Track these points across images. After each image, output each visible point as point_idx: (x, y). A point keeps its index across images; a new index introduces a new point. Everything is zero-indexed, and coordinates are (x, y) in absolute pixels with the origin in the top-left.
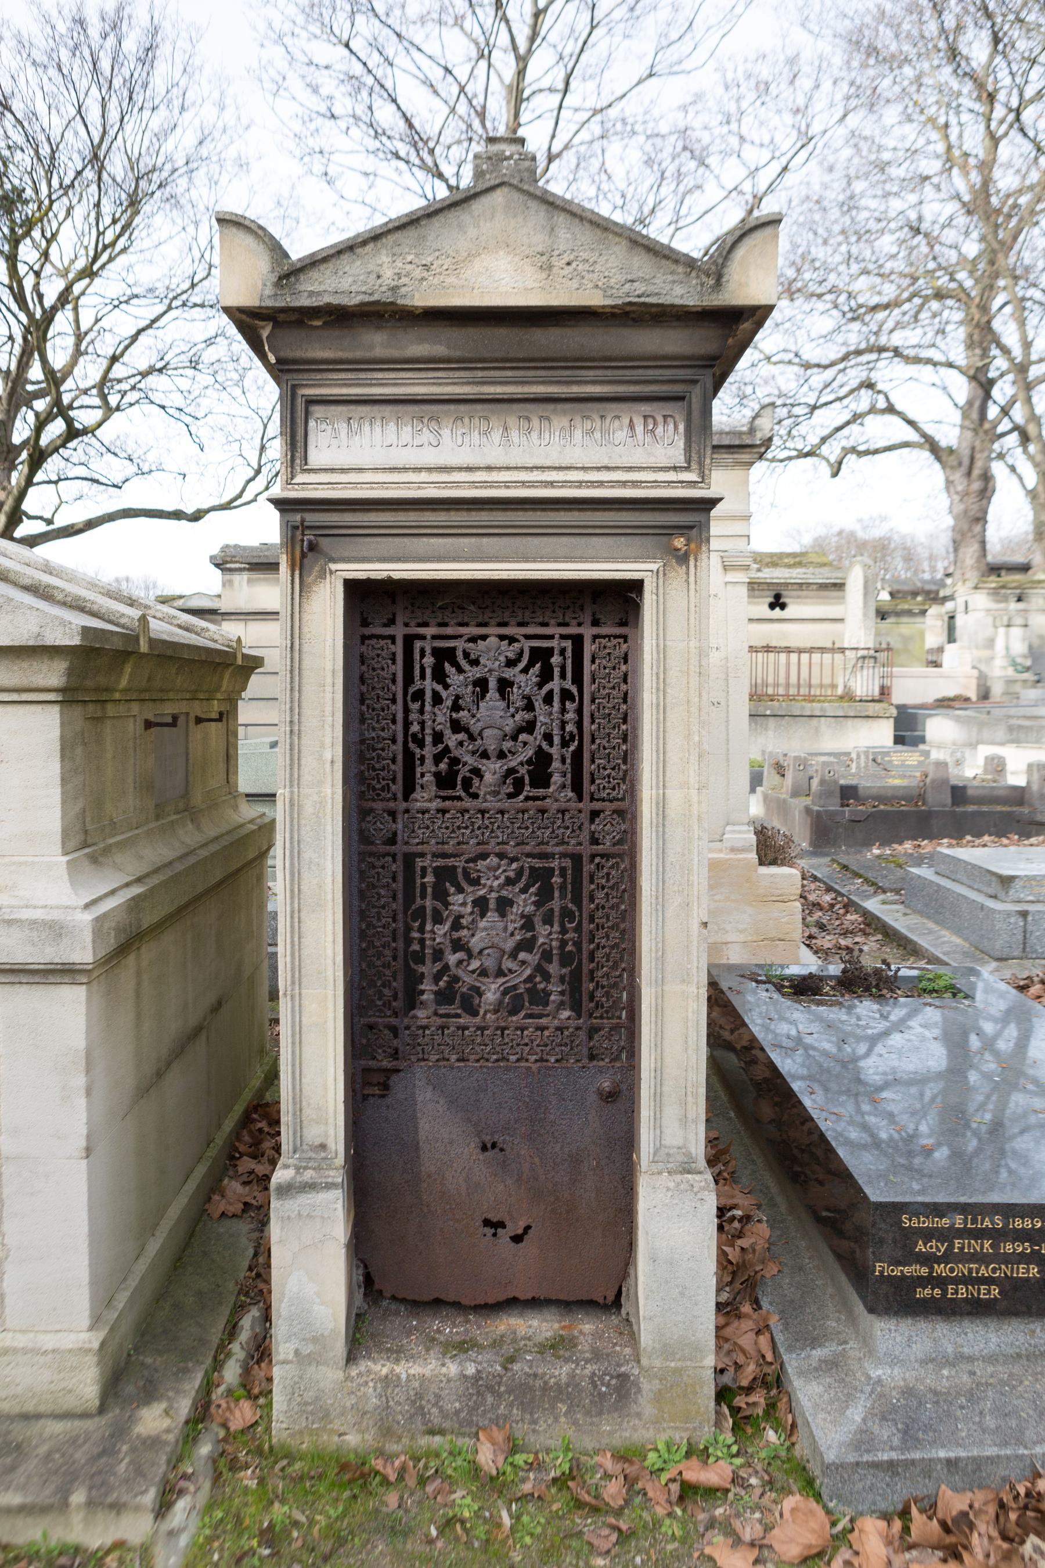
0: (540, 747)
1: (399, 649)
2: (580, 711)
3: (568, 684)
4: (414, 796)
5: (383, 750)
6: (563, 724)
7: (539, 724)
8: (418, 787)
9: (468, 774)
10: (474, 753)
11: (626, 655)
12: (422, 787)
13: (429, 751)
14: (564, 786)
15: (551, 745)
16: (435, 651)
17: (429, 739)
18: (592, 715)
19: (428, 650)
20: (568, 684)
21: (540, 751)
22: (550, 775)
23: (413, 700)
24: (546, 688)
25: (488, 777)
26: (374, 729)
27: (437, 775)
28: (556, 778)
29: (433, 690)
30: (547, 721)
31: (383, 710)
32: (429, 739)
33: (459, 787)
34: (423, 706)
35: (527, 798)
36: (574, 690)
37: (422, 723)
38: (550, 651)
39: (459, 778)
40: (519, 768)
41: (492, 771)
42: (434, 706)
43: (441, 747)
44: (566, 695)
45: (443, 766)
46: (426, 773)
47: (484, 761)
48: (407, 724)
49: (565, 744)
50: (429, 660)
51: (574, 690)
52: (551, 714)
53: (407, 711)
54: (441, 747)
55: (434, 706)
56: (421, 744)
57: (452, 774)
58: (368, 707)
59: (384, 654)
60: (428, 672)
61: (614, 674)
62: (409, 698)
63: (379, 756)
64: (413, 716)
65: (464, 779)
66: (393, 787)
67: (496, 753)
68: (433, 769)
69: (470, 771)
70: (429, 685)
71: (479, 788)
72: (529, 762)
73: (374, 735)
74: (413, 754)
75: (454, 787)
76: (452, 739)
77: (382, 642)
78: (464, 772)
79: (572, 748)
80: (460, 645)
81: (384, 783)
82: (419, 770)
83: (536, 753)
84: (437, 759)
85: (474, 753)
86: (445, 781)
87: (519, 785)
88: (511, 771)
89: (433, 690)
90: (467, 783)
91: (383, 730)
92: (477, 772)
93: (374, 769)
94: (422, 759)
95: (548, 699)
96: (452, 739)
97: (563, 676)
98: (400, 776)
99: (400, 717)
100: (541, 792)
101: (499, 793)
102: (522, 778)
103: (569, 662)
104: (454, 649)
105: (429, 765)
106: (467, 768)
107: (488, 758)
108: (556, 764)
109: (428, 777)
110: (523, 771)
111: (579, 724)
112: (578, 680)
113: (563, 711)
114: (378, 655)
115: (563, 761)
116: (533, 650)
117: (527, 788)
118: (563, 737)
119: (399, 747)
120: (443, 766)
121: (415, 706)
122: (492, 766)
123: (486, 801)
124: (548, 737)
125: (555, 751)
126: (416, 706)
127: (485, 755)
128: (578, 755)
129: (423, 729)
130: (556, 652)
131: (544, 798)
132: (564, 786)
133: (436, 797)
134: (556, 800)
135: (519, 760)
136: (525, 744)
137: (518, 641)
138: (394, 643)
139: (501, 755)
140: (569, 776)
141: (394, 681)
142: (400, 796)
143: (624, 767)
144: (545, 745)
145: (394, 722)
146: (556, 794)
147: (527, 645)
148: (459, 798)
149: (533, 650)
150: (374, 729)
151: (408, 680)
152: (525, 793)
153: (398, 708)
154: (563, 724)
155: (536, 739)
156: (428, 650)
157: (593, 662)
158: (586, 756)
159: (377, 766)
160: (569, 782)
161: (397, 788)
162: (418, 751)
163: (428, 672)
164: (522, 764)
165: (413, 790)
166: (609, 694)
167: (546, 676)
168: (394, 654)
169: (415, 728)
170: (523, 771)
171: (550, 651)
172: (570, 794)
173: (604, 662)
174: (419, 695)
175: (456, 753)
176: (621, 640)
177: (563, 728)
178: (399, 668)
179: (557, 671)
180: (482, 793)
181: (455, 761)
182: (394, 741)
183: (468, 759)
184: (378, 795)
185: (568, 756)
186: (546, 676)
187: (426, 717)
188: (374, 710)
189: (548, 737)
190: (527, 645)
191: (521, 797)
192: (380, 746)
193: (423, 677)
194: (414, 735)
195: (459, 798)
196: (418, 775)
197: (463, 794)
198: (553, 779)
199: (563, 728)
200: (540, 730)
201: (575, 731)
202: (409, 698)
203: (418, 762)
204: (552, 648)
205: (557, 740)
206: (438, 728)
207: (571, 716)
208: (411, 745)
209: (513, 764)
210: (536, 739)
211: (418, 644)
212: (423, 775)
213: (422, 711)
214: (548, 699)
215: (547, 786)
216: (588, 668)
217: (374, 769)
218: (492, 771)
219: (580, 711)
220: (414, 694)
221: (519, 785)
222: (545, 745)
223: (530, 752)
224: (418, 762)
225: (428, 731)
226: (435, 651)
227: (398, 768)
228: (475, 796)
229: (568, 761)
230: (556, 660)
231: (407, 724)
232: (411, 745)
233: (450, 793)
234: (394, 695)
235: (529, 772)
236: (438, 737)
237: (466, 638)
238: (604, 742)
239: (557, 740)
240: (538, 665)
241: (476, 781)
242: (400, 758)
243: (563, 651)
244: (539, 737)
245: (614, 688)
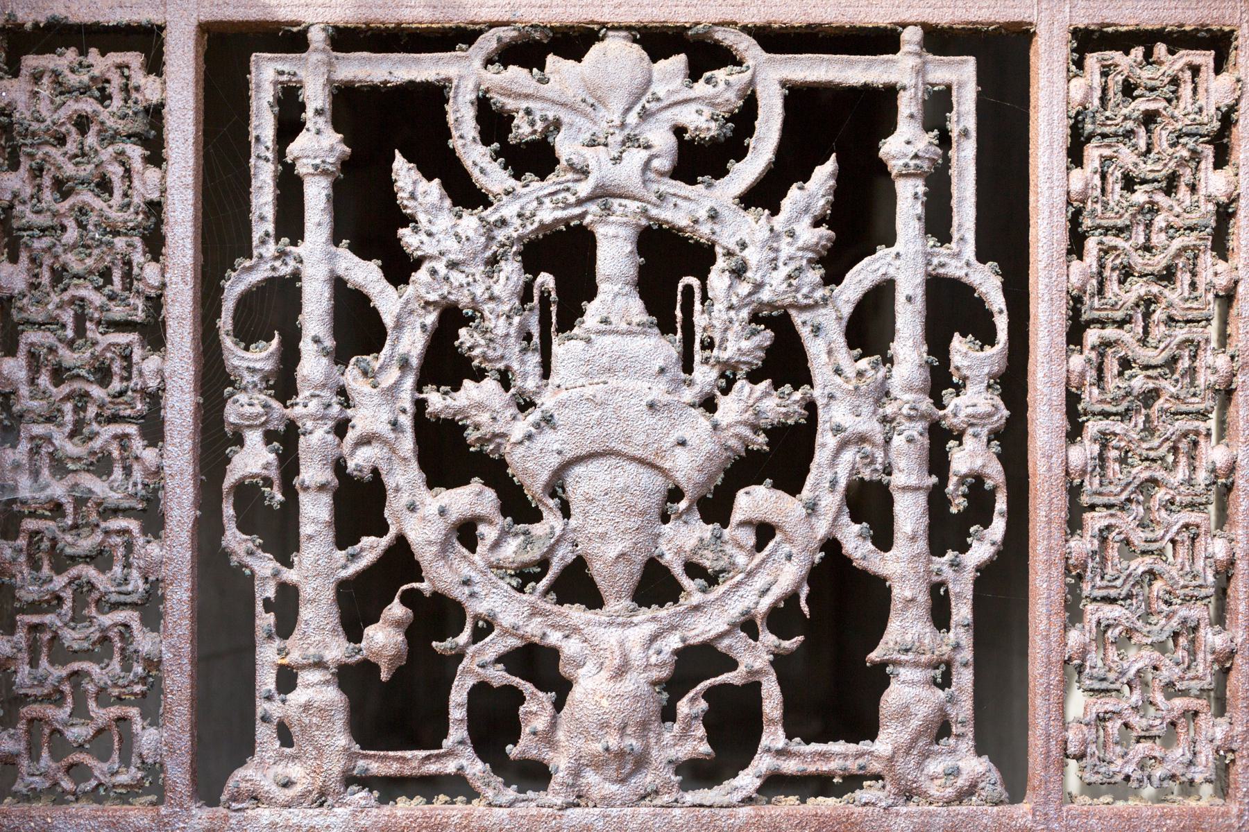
0: (831, 546)
1: (179, 90)
2: (1012, 383)
3: (962, 260)
4: (246, 775)
5: (100, 558)
6: (940, 440)
7: (826, 441)
8: (265, 734)
9: (499, 676)
10: (525, 576)
11: (1227, 119)
12: (285, 735)
13: (319, 565)
14: (942, 729)
15: (883, 539)
16: (350, 105)
17: (316, 512)
18: (1072, 400)
19: (315, 96)
20: (962, 260)
21: (832, 568)
22: (880, 678)
23: (247, 335)
24: (861, 278)
25: (591, 688)
26: (59, 466)
27: (355, 678)
28: (907, 696)
29: (339, 285)
30: (869, 425)
31: (103, 374)
32: (316, 512)
33: (457, 733)
34: (290, 356)
35: (775, 784)
36: (988, 284)
37: (286, 440)
38: (876, 107)
39: (458, 696)
40: (737, 645)
41: (613, 654)
42: (340, 357)
43: (371, 548)
44: (951, 309)
45: (384, 638)
46: (307, 665)
47: (576, 613)
48: (215, 442)
49: (946, 532)
50: (319, 145)
51: (988, 284)
52: (883, 394)
53: (214, 380)
54: (371, 548)
55: (340, 357)
56: (282, 538)
57: (424, 672)
58: (34, 360)
59: (109, 115)
60: (316, 195)
61: (1172, 208)
62: (225, 322)
63: (83, 589)
64: (244, 406)
65: (480, 691)
66: (148, 738)
67: (628, 576)
68: (337, 650)
69: (510, 660)
70: (321, 261)
71: (548, 737)
72: (782, 617)
73: (58, 490)
74: (244, 582)
75: (429, 732)
76: (422, 513)
77: (101, 63)
78: (480, 664)
79: (981, 550)
80: (464, 75)
81: (102, 715)
82: (268, 655)
83: (814, 575)
84: (357, 604)
85: (525, 576)
86: (394, 709)
87: (734, 726)
88: (697, 661)
89: (339, 285)
90: (495, 722)
91: (101, 465)
92: (539, 664)
93: (60, 654)
94: (287, 603)
95: (869, 328)
96: (422, 513)
97: (937, 222)
98: (178, 684)
99: (180, 407)
100: (838, 755)
101: (641, 762)
102: (753, 689)
103: (965, 157)
104: (433, 96)
105: (320, 635)
106: (495, 645)
107: (594, 600)
108: (905, 629)
109: (317, 692)
110: (754, 658)
111: (1012, 441)
112: (1005, 238)
113: (940, 380)
114: (82, 124)
115: (940, 614)
116: (800, 99)
117: (774, 737)
118: (937, 500)
119: (174, 550)
120: (384, 638)
121: (251, 360)
122: (610, 637)
123: (579, 799)
124: (869, 503)
125: (901, 566)
126: (260, 357)
127: (577, 586)
128: (1003, 585)
129: (289, 464)
130: (907, 105)
131: (853, 781)
132: (942, 729)
133: (350, 780)
134: (908, 794)
135: (735, 608)
136: (765, 532)
137: (726, 57)
138: (155, 66)
139: (655, 586)
140: (964, 678)
141: (155, 243)
142: (178, 775)
143: (1213, 639)
144: (855, 542)
145: (154, 431)
146: (907, 766)
147: (773, 75)
148: (458, 786)
149: (800, 99)
150: (59, 466)
151: (223, 235)
152: (762, 763)
153: (176, 366)
154: (940, 440)
155: (807, 516)
156: (315, 96)
157: (1075, 156)
158: (1044, 586)
159: (72, 638)
160: (964, 710)
161: (166, 739)
162: (264, 566)
163: (316, 195)
164: (748, 626)
165: (244, 749)
166: (1148, 303)
167: (857, 224)
168: (155, 113)
169: (253, 459)
170: (754, 658)
171: (876, 107)
172: (974, 765)
173: (1126, 156)
174: (274, 308)
175: (443, 573)
176: (1205, 58)
177: (938, 462)
178: (179, 182)
179: (908, 201)
180: (560, 763)
181: (438, 615)
182: (152, 517)
183: (496, 601)
184: (77, 771)
185: (962, 590)
186: (857, 224)
187: (305, 407)
188: (59, 374)
189: (869, 503)
190: (773, 75)
191: (747, 780)
192: (87, 543)
193: (290, 222)
194: (247, 492)
195: (458, 786)
196: (267, 680)
197: (475, 768)
198: (894, 696)
199: (938, 462)
200: (830, 470)
201: (995, 474)
202: (225, 322)
203: (265, 620)
204: (891, 92)
205: (909, 514)
206: (360, 460)
207: (975, 402)
208: (235, 540)
209: (704, 628)
210: (807, 516)
211: (266, 72)
212: (287, 679)
213: (283, 383)
214: (869, 328)
215: (863, 725)
216: (1049, 182)
217: (60, 654)
218: (613, 654)
219: (1012, 383)
220: (245, 301)
221: (734, 726)
222: (855, 542)
223: (786, 572)
224: (265, 620)
225: (313, 472)
226: (350, 105)
227: (172, 643)
228: (533, 775)
229: (962, 612)
230: (903, 145)
231: (215, 442)
232: (235, 540)
233: (413, 761)
234: (156, 303)
235: (780, 662)
236: (360, 504)
237: (488, 43)
238: (1126, 523)
239: (909, 514)
240: (824, 174)
241: (536, 708)
242: (179, 598)
243: (937, 106)
244: (831, 502)
245: (1168, 276)
